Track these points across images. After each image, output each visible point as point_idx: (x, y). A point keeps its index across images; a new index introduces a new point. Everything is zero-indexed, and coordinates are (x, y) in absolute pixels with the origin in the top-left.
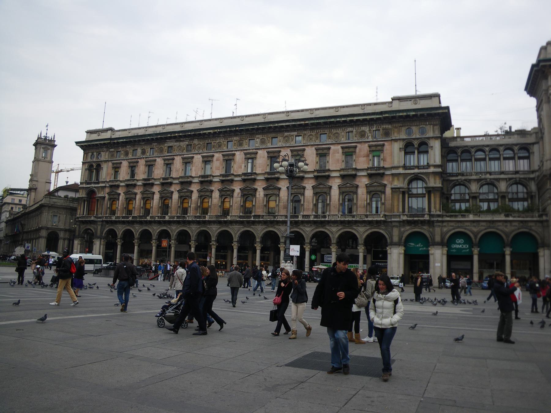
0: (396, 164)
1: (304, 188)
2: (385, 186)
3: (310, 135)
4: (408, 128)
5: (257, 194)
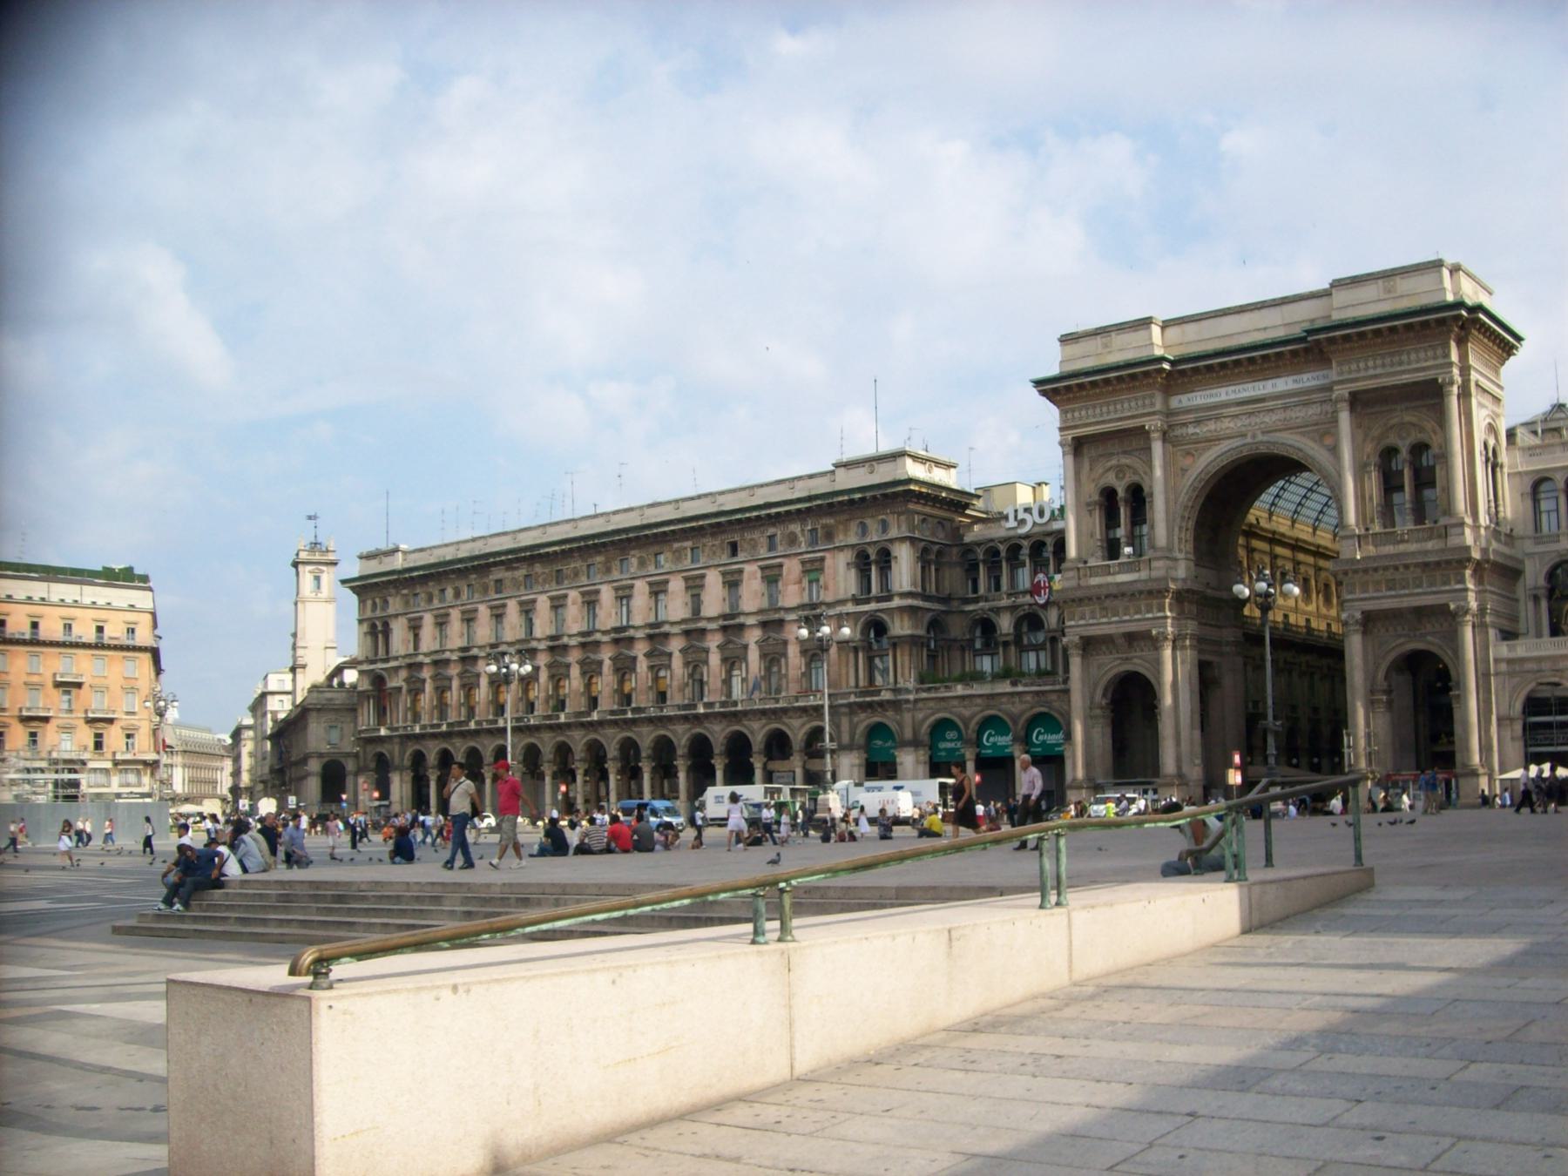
0: (841, 596)
1: (707, 651)
3: (713, 545)
4: (861, 523)
5: (638, 665)
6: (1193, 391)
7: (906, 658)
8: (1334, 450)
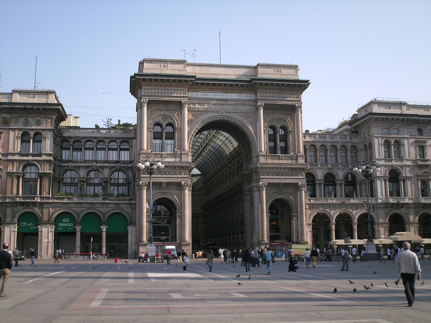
4: (25, 119)
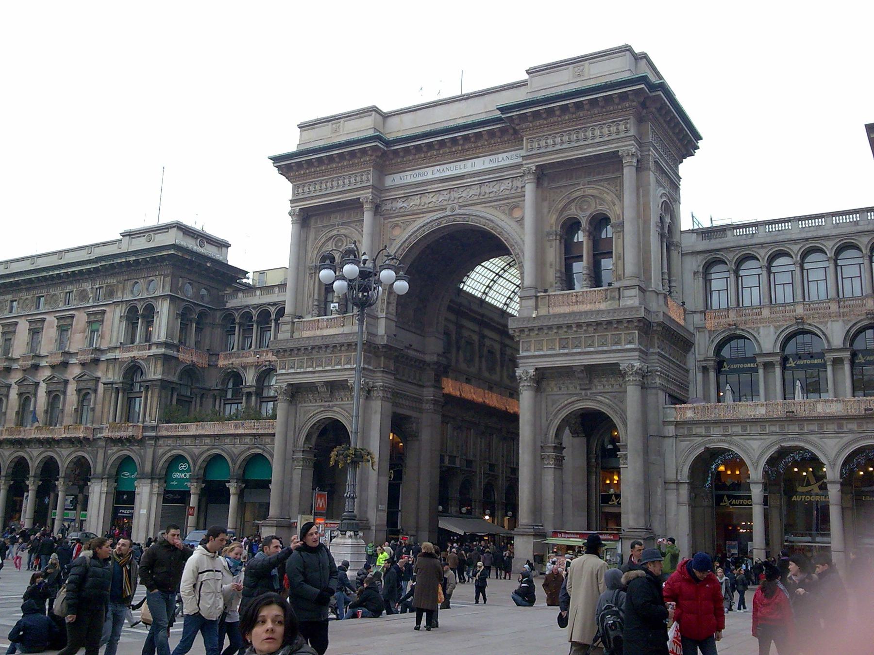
0: (113, 345)
2: (97, 379)
3: (27, 299)
6: (406, 171)
7: (155, 399)
8: (520, 221)
